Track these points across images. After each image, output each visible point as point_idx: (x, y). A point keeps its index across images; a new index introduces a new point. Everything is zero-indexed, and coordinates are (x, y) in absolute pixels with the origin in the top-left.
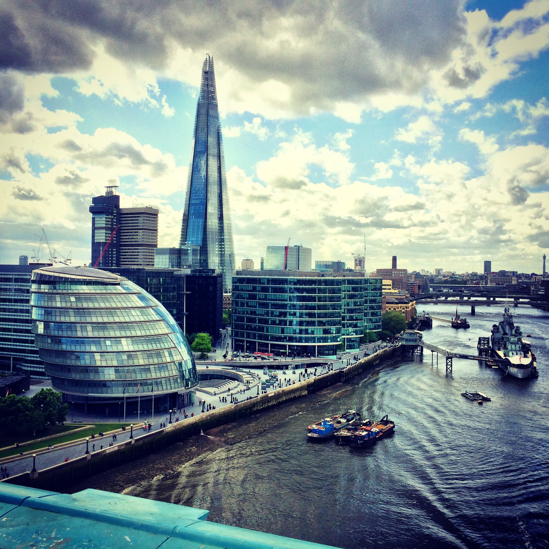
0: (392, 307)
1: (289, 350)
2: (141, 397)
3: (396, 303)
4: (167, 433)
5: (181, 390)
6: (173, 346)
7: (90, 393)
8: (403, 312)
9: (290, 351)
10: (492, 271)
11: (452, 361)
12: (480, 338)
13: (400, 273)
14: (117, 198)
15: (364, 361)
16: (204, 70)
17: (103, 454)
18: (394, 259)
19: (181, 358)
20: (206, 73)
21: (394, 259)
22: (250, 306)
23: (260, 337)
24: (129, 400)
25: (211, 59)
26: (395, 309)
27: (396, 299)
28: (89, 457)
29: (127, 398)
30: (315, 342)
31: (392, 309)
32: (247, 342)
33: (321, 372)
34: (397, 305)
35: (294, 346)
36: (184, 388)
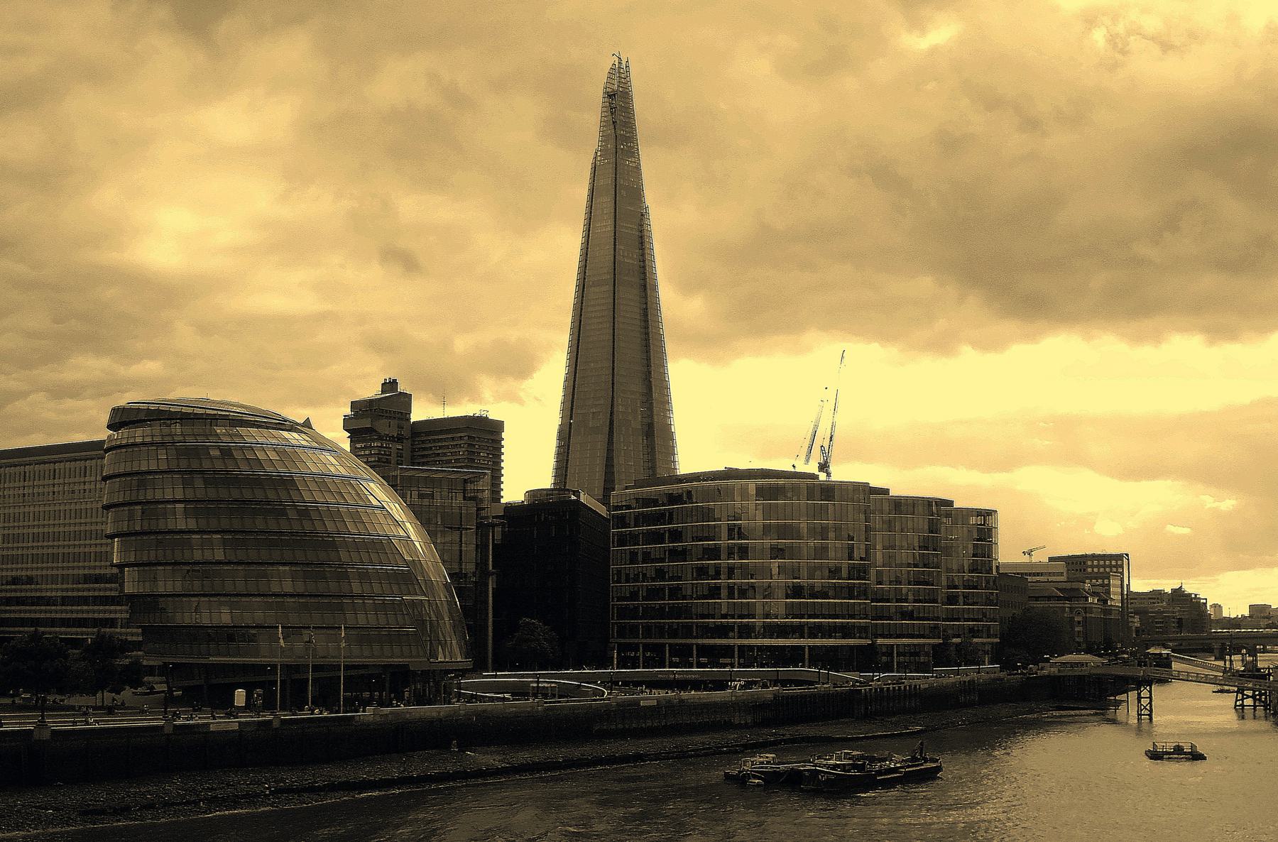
1: (739, 658)
3: (1059, 598)
7: (213, 656)
9: (742, 661)
13: (1113, 563)
15: (927, 686)
16: (608, 90)
20: (611, 96)
22: (653, 561)
23: (674, 633)
25: (624, 66)
27: (1057, 589)
32: (647, 647)
35: (751, 648)
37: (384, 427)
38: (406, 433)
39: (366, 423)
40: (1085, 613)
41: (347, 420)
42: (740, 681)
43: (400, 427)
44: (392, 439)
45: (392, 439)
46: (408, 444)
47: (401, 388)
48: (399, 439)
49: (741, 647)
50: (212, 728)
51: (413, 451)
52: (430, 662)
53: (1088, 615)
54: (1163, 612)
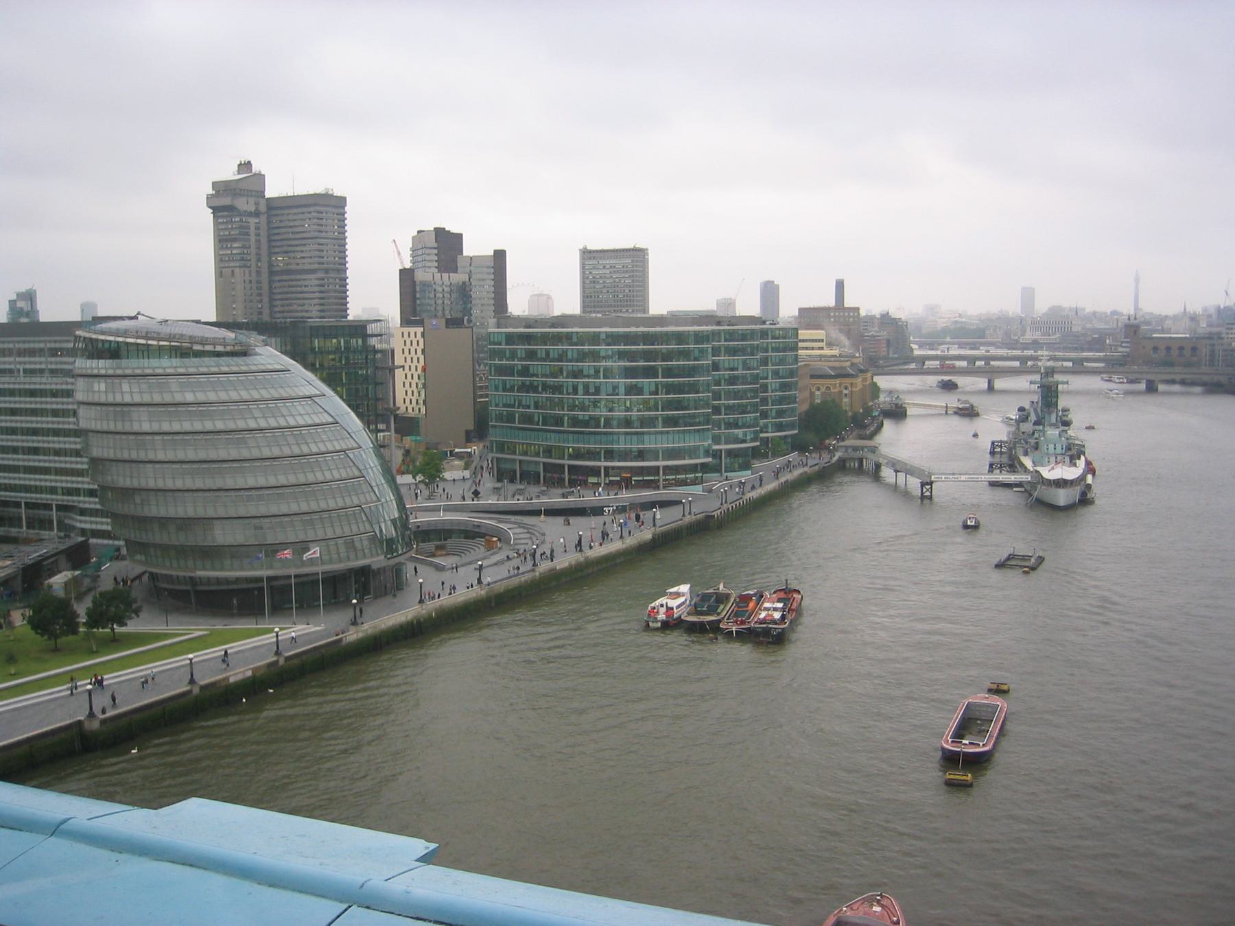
0: (823, 385)
2: (296, 576)
3: (831, 377)
4: (350, 644)
5: (377, 561)
6: (357, 473)
7: (200, 570)
8: (846, 395)
10: (845, 306)
11: (931, 488)
12: (993, 443)
14: (260, 177)
17: (223, 684)
18: (840, 286)
19: (374, 499)
21: (840, 286)
24: (275, 583)
26: (828, 388)
27: (830, 368)
28: (196, 690)
29: (270, 579)
30: (657, 459)
31: (823, 389)
33: (665, 519)
34: (832, 381)
36: (383, 557)
37: (243, 204)
38: (263, 208)
39: (226, 201)
40: (852, 387)
41: (209, 198)
42: (612, 506)
43: (257, 204)
44: (250, 214)
45: (250, 214)
46: (263, 219)
47: (255, 169)
48: (257, 214)
49: (606, 468)
50: (232, 680)
51: (269, 222)
52: (388, 559)
53: (854, 389)
54: (875, 336)
